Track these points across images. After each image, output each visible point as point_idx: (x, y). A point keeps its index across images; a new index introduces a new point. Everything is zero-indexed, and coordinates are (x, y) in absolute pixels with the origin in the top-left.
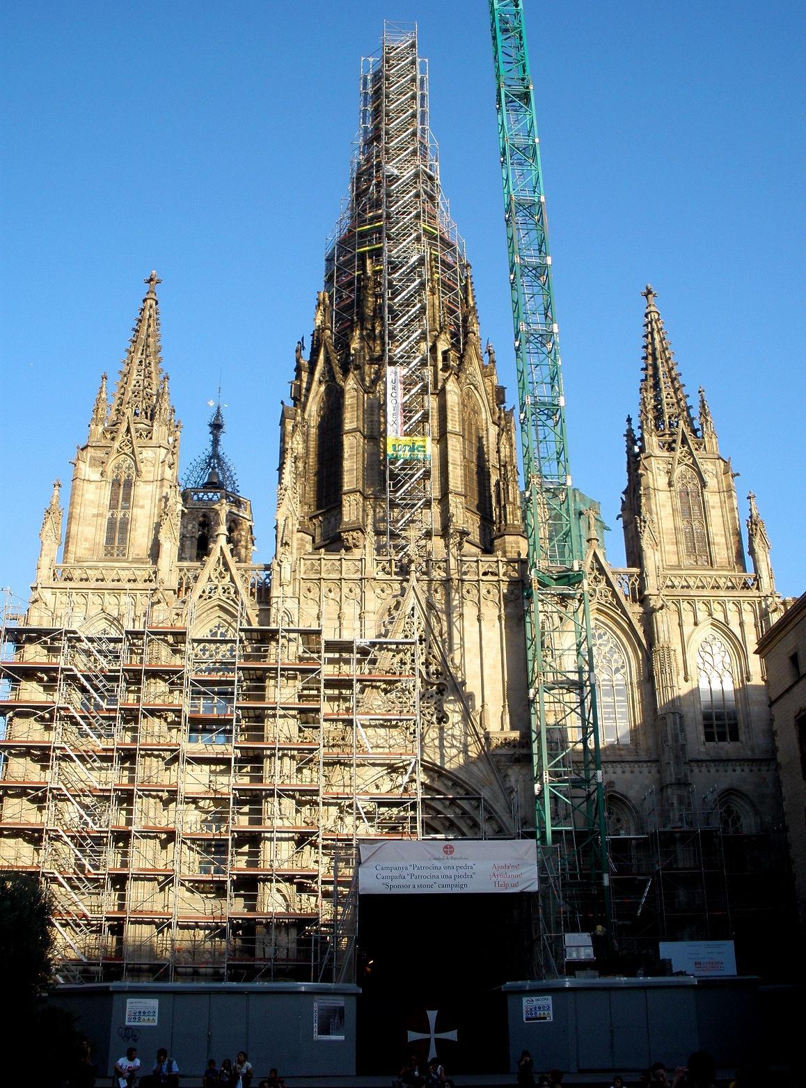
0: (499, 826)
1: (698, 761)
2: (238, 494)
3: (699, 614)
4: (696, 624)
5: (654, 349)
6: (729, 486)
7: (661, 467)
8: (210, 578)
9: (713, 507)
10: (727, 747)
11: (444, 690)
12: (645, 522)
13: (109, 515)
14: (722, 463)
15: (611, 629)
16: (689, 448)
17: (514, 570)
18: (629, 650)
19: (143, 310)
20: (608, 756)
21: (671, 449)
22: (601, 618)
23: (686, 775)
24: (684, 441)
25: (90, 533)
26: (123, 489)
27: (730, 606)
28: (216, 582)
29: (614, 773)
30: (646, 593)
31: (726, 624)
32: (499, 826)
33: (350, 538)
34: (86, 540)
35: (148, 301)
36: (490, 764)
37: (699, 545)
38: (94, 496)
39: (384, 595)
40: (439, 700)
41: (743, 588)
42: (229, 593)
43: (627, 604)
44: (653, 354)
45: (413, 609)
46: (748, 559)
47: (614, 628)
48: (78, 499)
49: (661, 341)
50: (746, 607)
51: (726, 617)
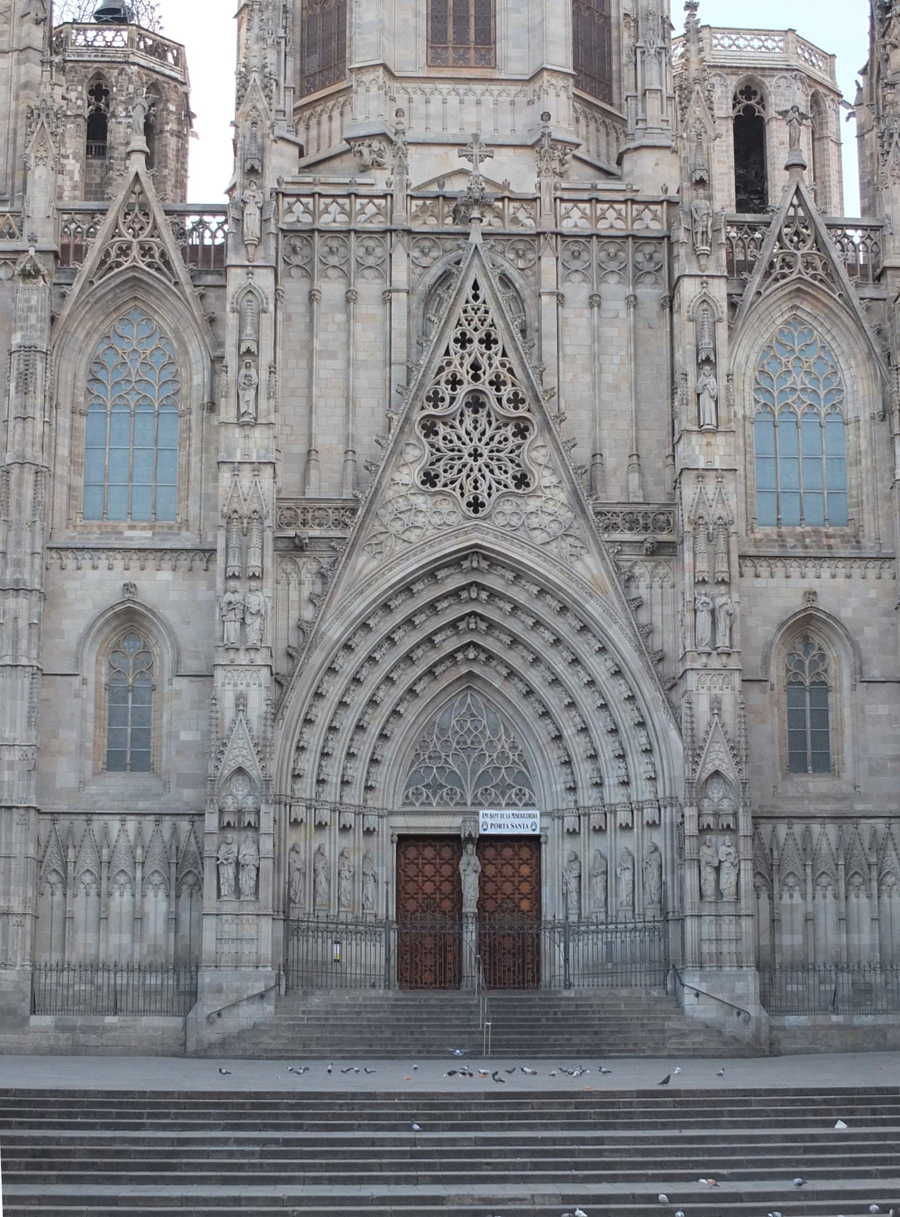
2: (161, 33)
8: (117, 227)
12: (891, 135)
17: (655, 218)
20: (806, 547)
29: (819, 577)
30: (887, 263)
33: (365, 151)
36: (603, 559)
39: (425, 261)
40: (519, 447)
42: (152, 257)
45: (476, 286)
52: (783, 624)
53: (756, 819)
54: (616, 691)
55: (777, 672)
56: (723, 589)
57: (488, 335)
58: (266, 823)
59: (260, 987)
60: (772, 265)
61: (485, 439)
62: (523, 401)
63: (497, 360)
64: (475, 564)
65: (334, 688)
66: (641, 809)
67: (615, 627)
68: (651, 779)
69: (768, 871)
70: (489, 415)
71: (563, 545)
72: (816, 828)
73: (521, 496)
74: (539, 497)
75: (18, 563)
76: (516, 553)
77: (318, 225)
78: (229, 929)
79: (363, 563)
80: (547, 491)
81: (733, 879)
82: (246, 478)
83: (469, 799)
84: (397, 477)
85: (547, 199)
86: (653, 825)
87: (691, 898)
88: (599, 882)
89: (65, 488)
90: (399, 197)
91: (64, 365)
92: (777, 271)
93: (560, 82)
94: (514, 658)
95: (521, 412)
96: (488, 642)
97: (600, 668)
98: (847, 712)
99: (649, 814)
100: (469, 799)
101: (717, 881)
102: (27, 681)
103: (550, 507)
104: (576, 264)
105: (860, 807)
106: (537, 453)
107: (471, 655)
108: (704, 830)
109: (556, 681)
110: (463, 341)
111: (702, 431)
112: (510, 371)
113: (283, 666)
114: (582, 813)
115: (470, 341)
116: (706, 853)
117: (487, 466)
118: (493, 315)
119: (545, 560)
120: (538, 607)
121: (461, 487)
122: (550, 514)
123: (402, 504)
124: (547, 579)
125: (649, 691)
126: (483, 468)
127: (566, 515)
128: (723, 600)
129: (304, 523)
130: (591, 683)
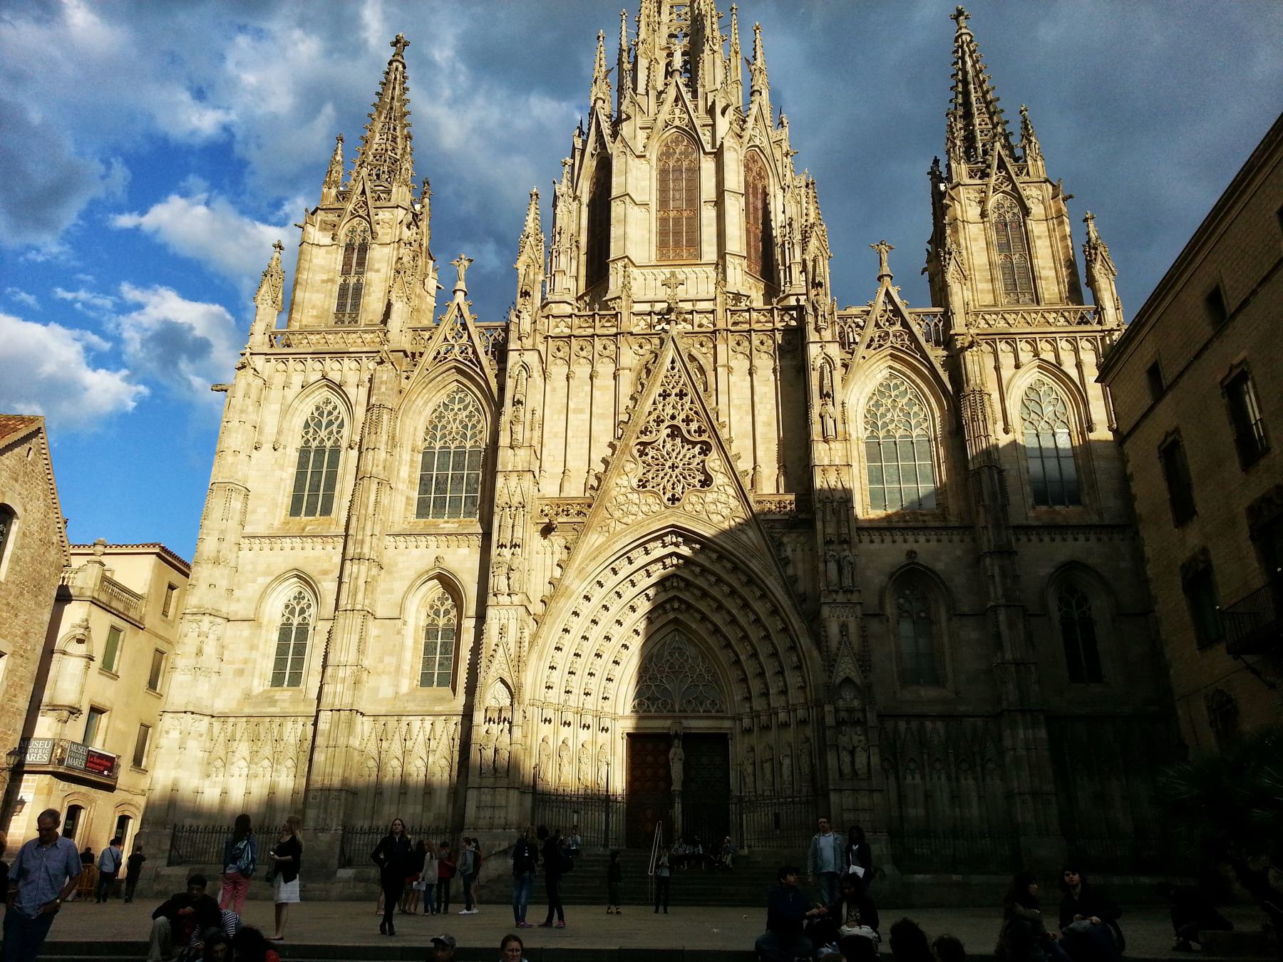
0: (774, 605)
1: (1027, 529)
3: (1021, 354)
4: (1017, 366)
5: (965, 73)
6: (1059, 211)
7: (972, 197)
8: (445, 338)
9: (1039, 237)
10: (1065, 512)
13: (341, 280)
14: (1050, 187)
15: (909, 378)
16: (1008, 173)
17: (792, 318)
18: (932, 400)
19: (388, 73)
20: (906, 521)
21: (985, 175)
22: (897, 366)
23: (1009, 542)
24: (1002, 165)
25: (317, 300)
26: (357, 254)
27: (1063, 344)
28: (452, 342)
29: (917, 541)
31: (1058, 365)
32: (774, 605)
34: (313, 307)
35: (395, 64)
37: (1020, 280)
38: (324, 261)
39: (641, 351)
41: (1079, 323)
43: (928, 347)
44: (965, 83)
45: (673, 362)
46: (1086, 292)
47: (914, 376)
48: (305, 265)
49: (974, 66)
50: (1084, 344)
51: (1057, 356)
52: (892, 574)
53: (881, 717)
54: (774, 625)
55: (890, 610)
56: (845, 546)
57: (681, 391)
58: (518, 718)
59: (505, 845)
60: (872, 340)
61: (680, 456)
62: (704, 431)
63: (687, 406)
64: (674, 540)
65: (578, 626)
66: (795, 710)
67: (771, 578)
68: (802, 688)
69: (893, 758)
72: (929, 725)
73: (705, 492)
75: (362, 542)
77: (575, 333)
78: (487, 798)
79: (594, 539)
81: (865, 761)
82: (513, 479)
83: (677, 708)
84: (619, 481)
86: (803, 722)
87: (833, 775)
88: (767, 766)
89: (404, 499)
90: (625, 314)
91: (408, 421)
92: (875, 344)
93: (737, 261)
94: (703, 606)
95: (705, 437)
96: (686, 596)
97: (760, 607)
98: (946, 639)
99: (801, 713)
100: (677, 708)
101: (853, 762)
102: (359, 621)
103: (723, 498)
104: (739, 349)
105: (962, 709)
106: (714, 462)
107: (676, 606)
108: (840, 723)
109: (734, 621)
110: (665, 395)
111: (826, 441)
112: (696, 413)
113: (537, 608)
114: (755, 715)
115: (669, 395)
116: (844, 740)
118: (684, 378)
120: (716, 568)
124: (722, 547)
125: (796, 622)
127: (734, 503)
128: (847, 553)
129: (557, 514)
130: (758, 620)
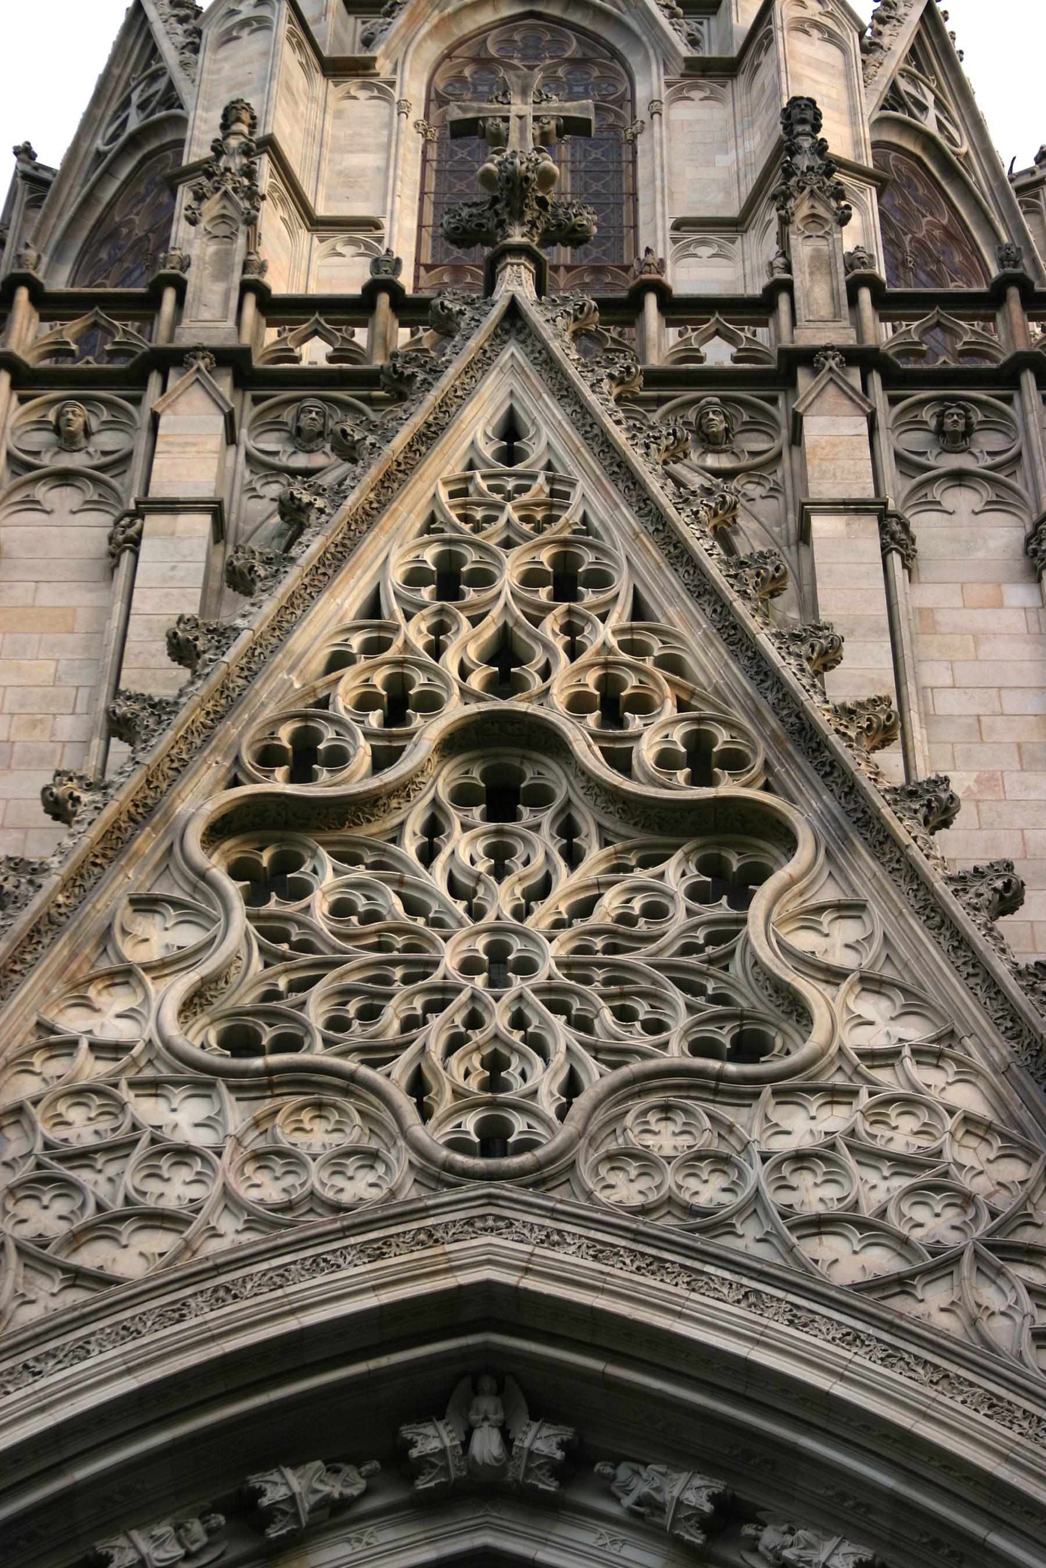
11: (759, 874)
45: (511, 431)
62: (735, 761)
63: (603, 634)
70: (568, 829)
71: (990, 1296)
74: (836, 1096)
76: (713, 1319)
80: (883, 1075)
84: (72, 1022)
85: (816, 292)
103: (902, 1135)
115: (483, 579)
117: (557, 1008)
118: (591, 498)
119: (891, 1356)
121: (418, 1086)
122: (902, 1163)
123: (82, 1127)
126: (537, 1010)
